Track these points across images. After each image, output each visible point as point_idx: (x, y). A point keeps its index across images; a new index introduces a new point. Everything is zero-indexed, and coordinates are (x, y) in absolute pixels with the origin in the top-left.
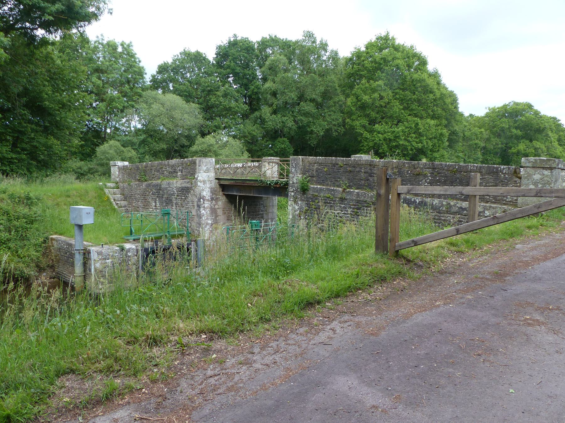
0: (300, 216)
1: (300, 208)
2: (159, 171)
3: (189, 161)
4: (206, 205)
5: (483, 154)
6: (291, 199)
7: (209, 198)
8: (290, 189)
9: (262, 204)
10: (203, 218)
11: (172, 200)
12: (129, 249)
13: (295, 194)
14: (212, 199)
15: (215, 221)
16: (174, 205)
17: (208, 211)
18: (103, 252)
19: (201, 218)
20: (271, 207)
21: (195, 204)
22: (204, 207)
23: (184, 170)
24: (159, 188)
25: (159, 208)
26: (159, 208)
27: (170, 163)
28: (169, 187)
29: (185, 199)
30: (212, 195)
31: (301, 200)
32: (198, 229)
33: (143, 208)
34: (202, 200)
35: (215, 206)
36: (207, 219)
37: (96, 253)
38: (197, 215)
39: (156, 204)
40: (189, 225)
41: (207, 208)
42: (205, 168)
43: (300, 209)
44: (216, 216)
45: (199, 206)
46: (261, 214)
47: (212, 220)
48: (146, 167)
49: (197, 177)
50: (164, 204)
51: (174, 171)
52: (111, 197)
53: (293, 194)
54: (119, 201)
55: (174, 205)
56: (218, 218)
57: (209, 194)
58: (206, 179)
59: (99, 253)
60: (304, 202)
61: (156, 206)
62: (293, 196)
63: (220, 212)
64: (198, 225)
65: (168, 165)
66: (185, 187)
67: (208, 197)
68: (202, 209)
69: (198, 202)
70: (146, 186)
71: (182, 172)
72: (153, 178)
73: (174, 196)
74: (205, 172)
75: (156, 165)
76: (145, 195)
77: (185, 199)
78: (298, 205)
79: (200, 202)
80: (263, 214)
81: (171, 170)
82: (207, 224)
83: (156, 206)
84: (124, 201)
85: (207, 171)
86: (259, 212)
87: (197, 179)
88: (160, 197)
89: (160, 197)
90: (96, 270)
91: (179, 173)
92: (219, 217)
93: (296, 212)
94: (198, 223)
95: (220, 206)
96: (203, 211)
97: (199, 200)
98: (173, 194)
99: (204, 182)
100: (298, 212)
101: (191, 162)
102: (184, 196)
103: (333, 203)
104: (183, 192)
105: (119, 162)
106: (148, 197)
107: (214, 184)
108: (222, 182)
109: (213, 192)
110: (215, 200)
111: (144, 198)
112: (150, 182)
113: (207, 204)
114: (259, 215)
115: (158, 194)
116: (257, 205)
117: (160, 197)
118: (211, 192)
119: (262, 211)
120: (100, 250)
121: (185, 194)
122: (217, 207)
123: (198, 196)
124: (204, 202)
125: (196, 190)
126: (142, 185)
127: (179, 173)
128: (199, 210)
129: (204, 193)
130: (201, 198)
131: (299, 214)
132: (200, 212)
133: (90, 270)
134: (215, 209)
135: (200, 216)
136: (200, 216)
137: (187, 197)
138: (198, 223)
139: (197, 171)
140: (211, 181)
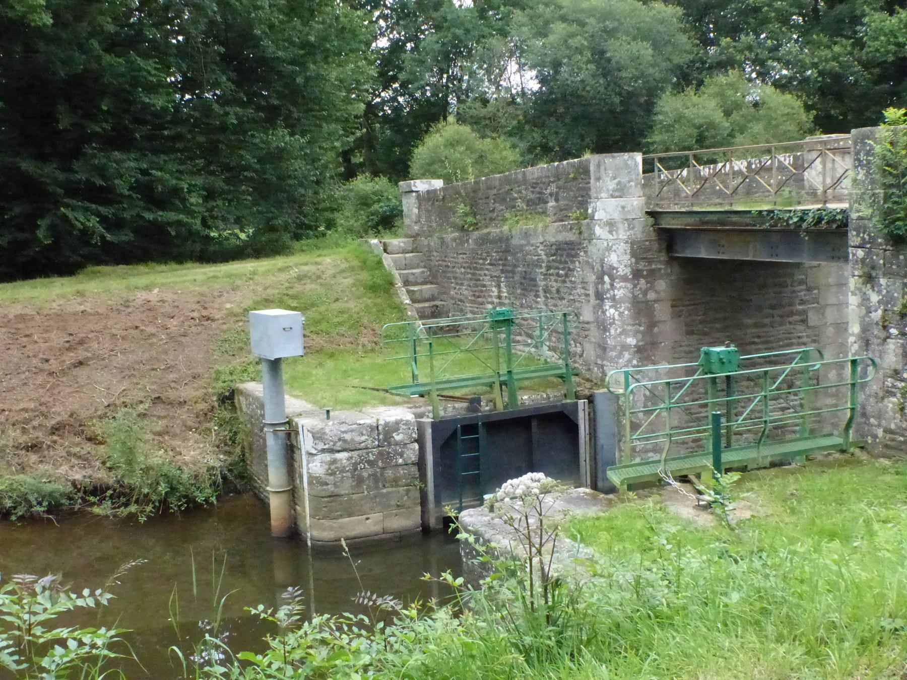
0: (885, 327)
1: (887, 301)
2: (504, 199)
3: (573, 165)
4: (619, 293)
5: (206, 199)
7: (628, 271)
8: (853, 238)
9: (801, 282)
10: (612, 331)
11: (535, 280)
12: (397, 423)
13: (869, 253)
14: (637, 274)
15: (648, 339)
16: (541, 293)
17: (625, 309)
18: (327, 431)
19: (605, 330)
20: (834, 289)
21: (591, 291)
22: (613, 298)
23: (561, 194)
24: (504, 246)
25: (507, 301)
26: (507, 301)
27: (529, 177)
28: (529, 244)
29: (566, 275)
30: (637, 263)
31: (888, 274)
32: (599, 362)
33: (472, 302)
34: (606, 278)
35: (645, 293)
36: (624, 332)
37: (310, 435)
38: (597, 321)
39: (500, 292)
40: (579, 350)
41: (621, 301)
42: (612, 185)
44: (652, 325)
45: (600, 296)
46: (800, 313)
47: (640, 336)
48: (474, 192)
49: (594, 213)
50: (519, 291)
51: (539, 199)
52: (396, 273)
53: (860, 253)
54: (416, 284)
55: (541, 293)
56: (656, 330)
57: (627, 259)
58: (616, 216)
59: (318, 436)
60: (898, 283)
61: (499, 297)
62: (863, 261)
63: (662, 311)
64: (599, 352)
65: (525, 181)
66: (566, 243)
67: (623, 270)
68: (607, 305)
69: (596, 284)
70: (476, 241)
71: (557, 200)
72: (492, 219)
73: (541, 267)
74: (612, 196)
75: (497, 183)
76: (476, 268)
77: (566, 275)
78: (879, 292)
79: (603, 283)
80: (805, 312)
81: (533, 196)
82: (625, 347)
83: (499, 297)
84: (432, 283)
85: (620, 192)
86: (791, 304)
87: (592, 218)
88: (508, 271)
89: (508, 271)
90: (310, 477)
91: (552, 203)
92: (661, 326)
93: (873, 315)
94: (599, 345)
95: (663, 295)
96: (612, 311)
97: (600, 279)
98: (538, 264)
99: (611, 225)
100: (880, 312)
101: (577, 170)
102: (563, 269)
104: (562, 256)
105: (418, 182)
106: (482, 273)
107: (641, 229)
108: (668, 223)
109: (638, 252)
110: (644, 277)
111: (473, 274)
112: (486, 231)
113: (621, 291)
114: (792, 314)
115: (504, 265)
116: (783, 285)
117: (509, 272)
118: (633, 254)
119: (803, 302)
120: (320, 425)
121: (566, 262)
122: (651, 296)
123: (597, 267)
124: (612, 285)
125: (592, 249)
126: (467, 241)
127: (552, 203)
128: (600, 306)
129: (613, 259)
130: (605, 271)
131: (884, 319)
132: (604, 312)
133: (301, 477)
134: (647, 302)
135: (603, 326)
136: (603, 324)
137: (570, 270)
138: (599, 345)
139: (593, 193)
140: (630, 222)
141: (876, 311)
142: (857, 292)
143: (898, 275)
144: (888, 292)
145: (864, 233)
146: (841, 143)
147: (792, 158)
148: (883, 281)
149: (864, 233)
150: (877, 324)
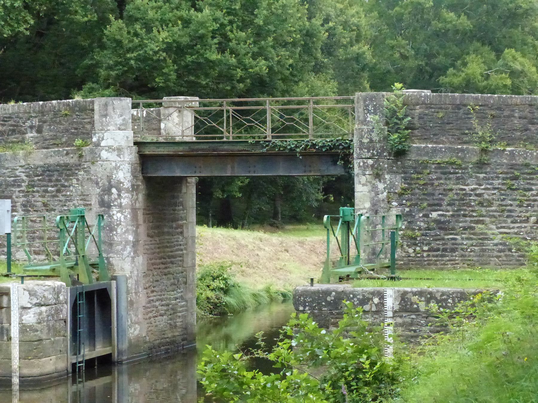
1: (390, 189)
6: (367, 173)
10: (119, 230)
17: (127, 212)
22: (120, 206)
29: (58, 191)
31: (391, 172)
34: (114, 190)
36: (127, 231)
37: (27, 293)
42: (119, 121)
43: (391, 188)
57: (129, 176)
60: (398, 177)
62: (372, 166)
67: (127, 185)
74: (119, 129)
78: (385, 183)
79: (110, 193)
82: (127, 242)
87: (98, 145)
91: (30, 135)
93: (380, 196)
96: (119, 215)
97: (107, 191)
103: (462, 173)
124: (119, 195)
131: (388, 197)
141: (382, 193)
142: (368, 184)
143: (397, 172)
144: (390, 182)
145: (373, 150)
146: (193, 103)
147: (145, 113)
148: (387, 177)
149: (373, 150)
150: (383, 200)
